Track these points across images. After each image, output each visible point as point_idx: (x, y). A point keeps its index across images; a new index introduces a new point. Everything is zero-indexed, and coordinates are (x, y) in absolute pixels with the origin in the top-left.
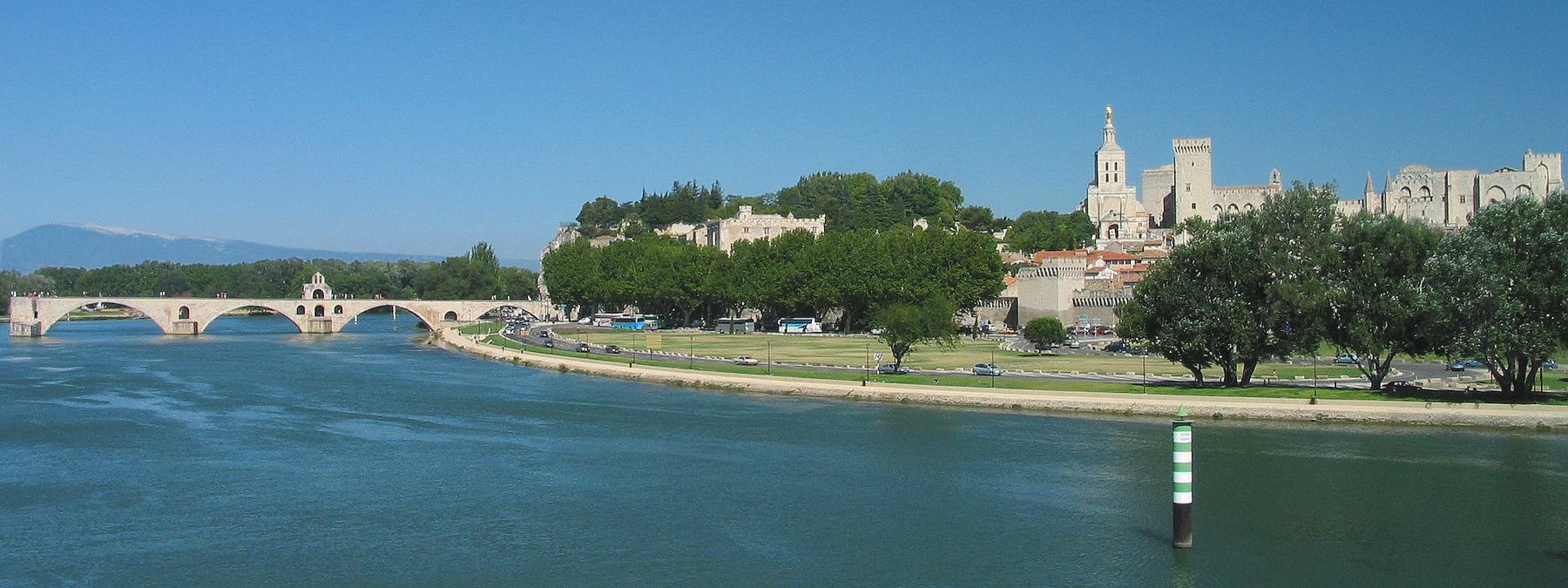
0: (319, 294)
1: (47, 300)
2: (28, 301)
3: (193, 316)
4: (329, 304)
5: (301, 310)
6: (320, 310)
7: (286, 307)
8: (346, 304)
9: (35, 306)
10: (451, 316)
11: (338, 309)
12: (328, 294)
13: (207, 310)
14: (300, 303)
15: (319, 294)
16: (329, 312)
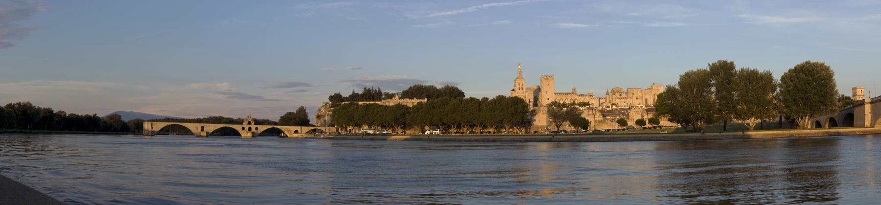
0: (249, 123)
3: (205, 130)
4: (253, 127)
5: (243, 129)
6: (250, 129)
8: (259, 127)
10: (296, 132)
11: (257, 129)
12: (253, 123)
16: (253, 129)
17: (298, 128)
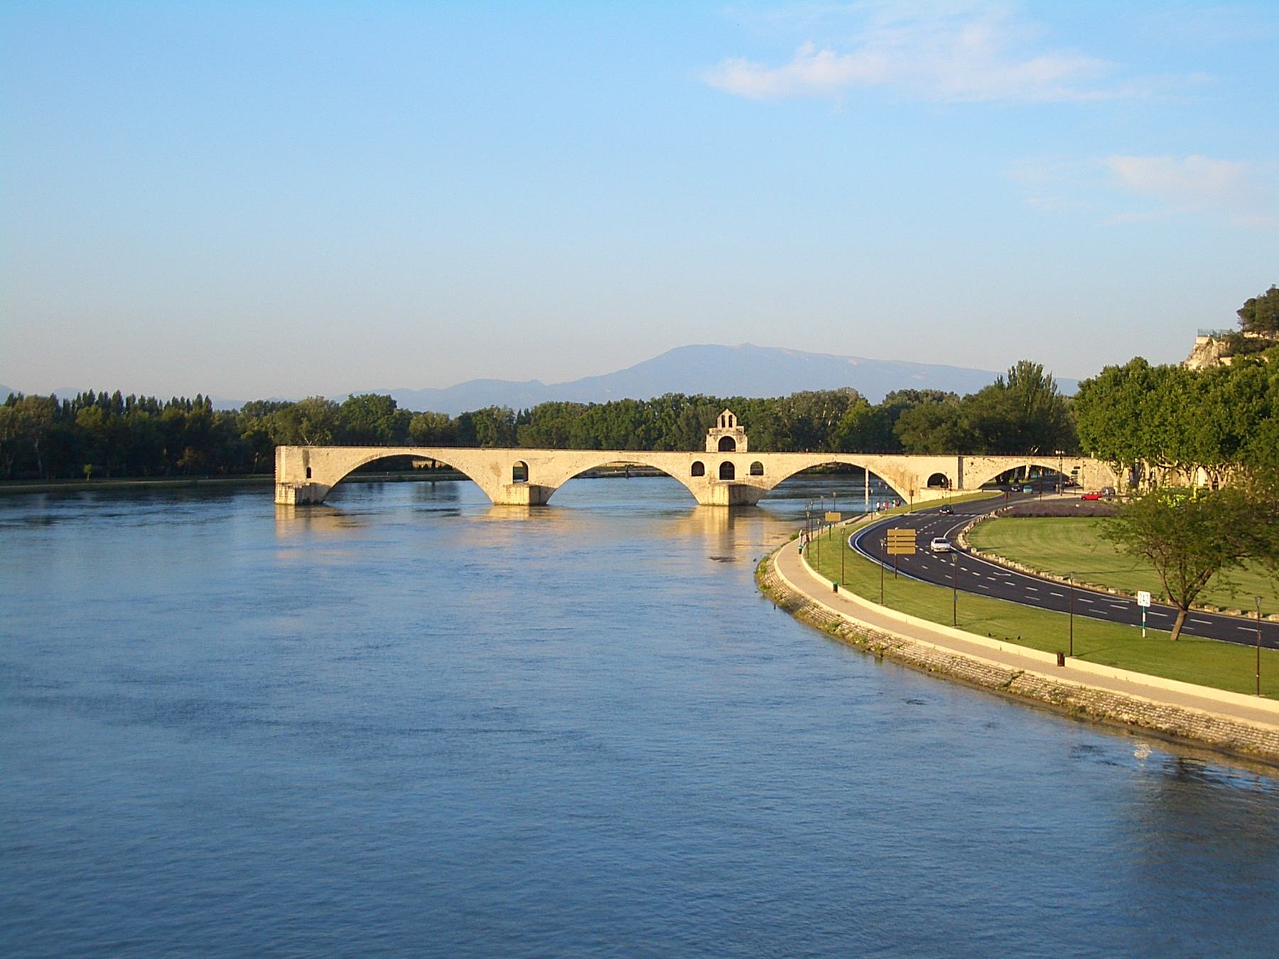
1: (324, 450)
2: (297, 451)
4: (742, 461)
5: (698, 469)
6: (727, 470)
7: (676, 463)
9: (306, 460)
11: (757, 470)
12: (742, 445)
13: (555, 467)
14: (697, 457)
15: (727, 445)
16: (742, 474)
17: (946, 465)
